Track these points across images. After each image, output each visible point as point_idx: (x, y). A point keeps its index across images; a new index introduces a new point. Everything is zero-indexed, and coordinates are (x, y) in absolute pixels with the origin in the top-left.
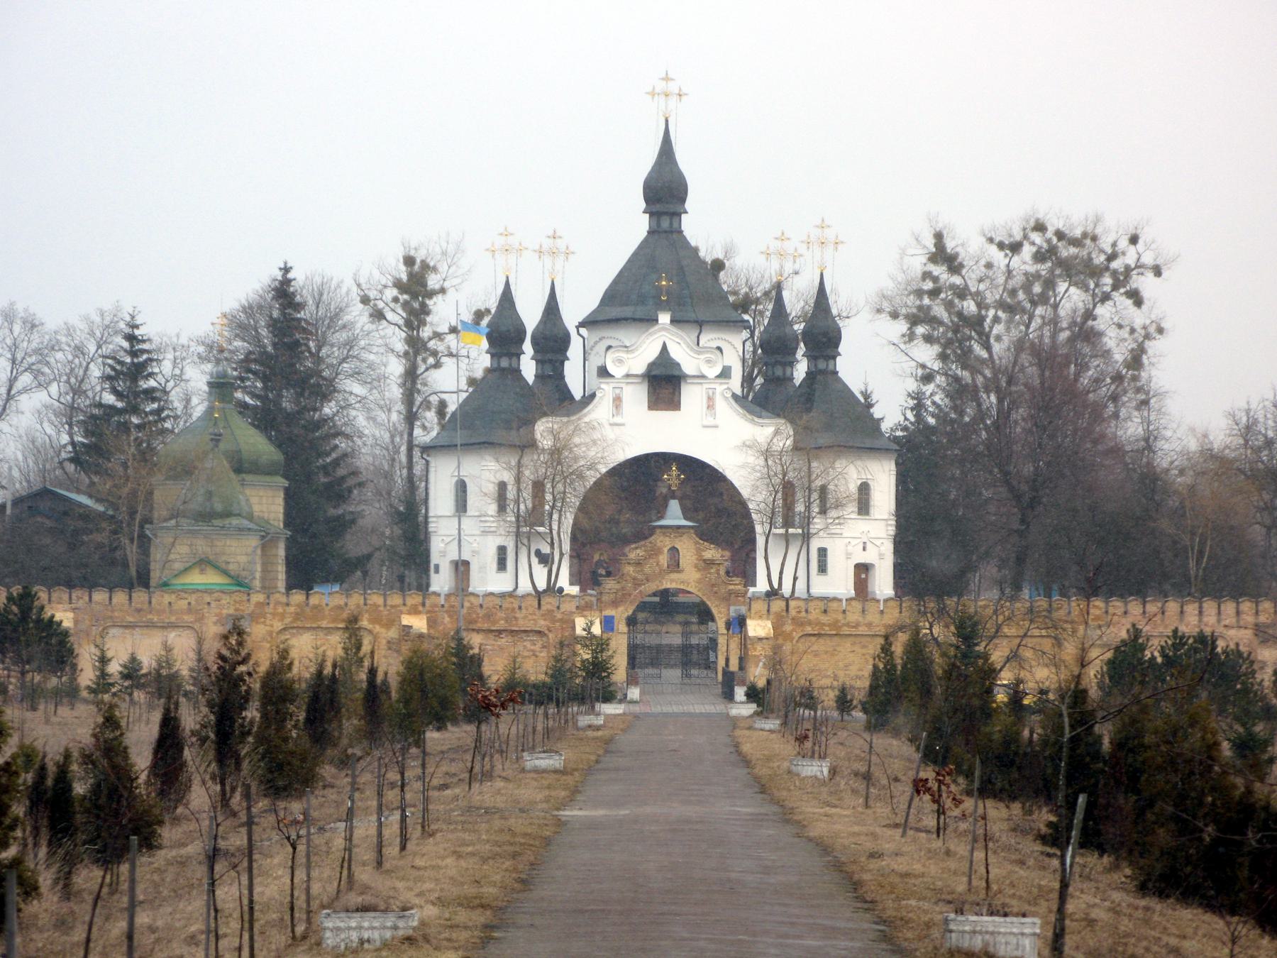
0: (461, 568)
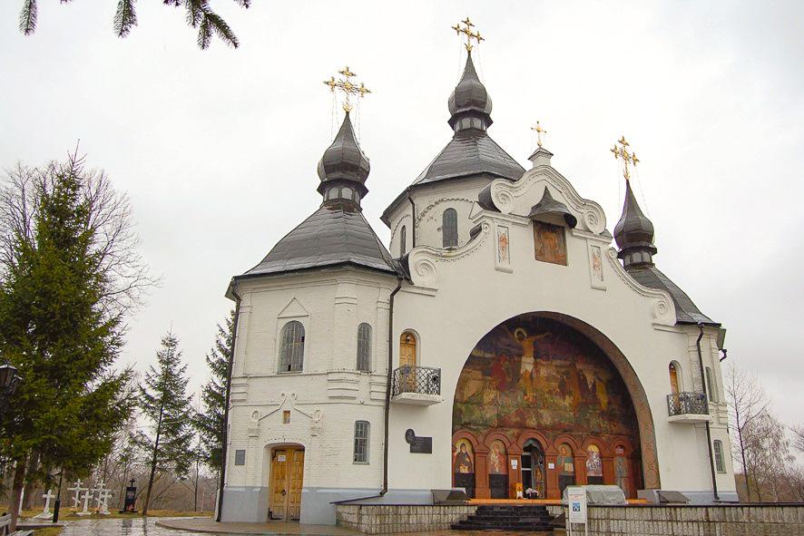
0: (287, 456)
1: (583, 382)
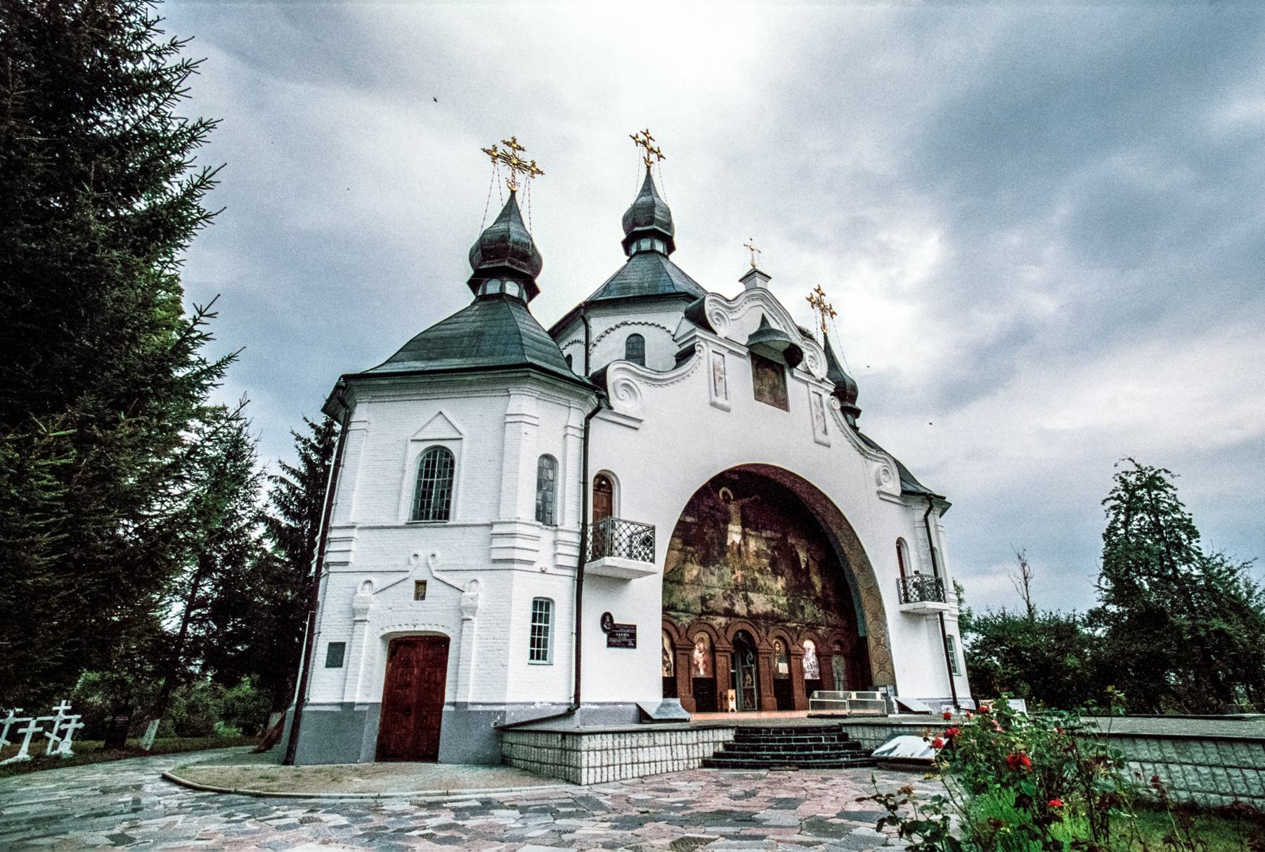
1: (796, 560)
